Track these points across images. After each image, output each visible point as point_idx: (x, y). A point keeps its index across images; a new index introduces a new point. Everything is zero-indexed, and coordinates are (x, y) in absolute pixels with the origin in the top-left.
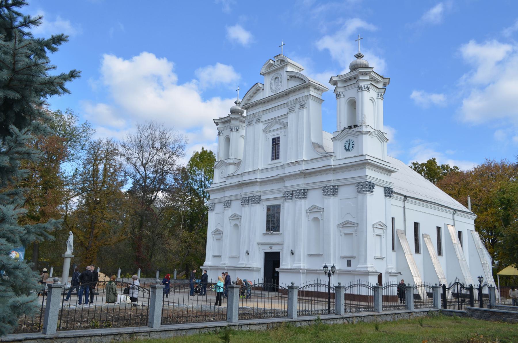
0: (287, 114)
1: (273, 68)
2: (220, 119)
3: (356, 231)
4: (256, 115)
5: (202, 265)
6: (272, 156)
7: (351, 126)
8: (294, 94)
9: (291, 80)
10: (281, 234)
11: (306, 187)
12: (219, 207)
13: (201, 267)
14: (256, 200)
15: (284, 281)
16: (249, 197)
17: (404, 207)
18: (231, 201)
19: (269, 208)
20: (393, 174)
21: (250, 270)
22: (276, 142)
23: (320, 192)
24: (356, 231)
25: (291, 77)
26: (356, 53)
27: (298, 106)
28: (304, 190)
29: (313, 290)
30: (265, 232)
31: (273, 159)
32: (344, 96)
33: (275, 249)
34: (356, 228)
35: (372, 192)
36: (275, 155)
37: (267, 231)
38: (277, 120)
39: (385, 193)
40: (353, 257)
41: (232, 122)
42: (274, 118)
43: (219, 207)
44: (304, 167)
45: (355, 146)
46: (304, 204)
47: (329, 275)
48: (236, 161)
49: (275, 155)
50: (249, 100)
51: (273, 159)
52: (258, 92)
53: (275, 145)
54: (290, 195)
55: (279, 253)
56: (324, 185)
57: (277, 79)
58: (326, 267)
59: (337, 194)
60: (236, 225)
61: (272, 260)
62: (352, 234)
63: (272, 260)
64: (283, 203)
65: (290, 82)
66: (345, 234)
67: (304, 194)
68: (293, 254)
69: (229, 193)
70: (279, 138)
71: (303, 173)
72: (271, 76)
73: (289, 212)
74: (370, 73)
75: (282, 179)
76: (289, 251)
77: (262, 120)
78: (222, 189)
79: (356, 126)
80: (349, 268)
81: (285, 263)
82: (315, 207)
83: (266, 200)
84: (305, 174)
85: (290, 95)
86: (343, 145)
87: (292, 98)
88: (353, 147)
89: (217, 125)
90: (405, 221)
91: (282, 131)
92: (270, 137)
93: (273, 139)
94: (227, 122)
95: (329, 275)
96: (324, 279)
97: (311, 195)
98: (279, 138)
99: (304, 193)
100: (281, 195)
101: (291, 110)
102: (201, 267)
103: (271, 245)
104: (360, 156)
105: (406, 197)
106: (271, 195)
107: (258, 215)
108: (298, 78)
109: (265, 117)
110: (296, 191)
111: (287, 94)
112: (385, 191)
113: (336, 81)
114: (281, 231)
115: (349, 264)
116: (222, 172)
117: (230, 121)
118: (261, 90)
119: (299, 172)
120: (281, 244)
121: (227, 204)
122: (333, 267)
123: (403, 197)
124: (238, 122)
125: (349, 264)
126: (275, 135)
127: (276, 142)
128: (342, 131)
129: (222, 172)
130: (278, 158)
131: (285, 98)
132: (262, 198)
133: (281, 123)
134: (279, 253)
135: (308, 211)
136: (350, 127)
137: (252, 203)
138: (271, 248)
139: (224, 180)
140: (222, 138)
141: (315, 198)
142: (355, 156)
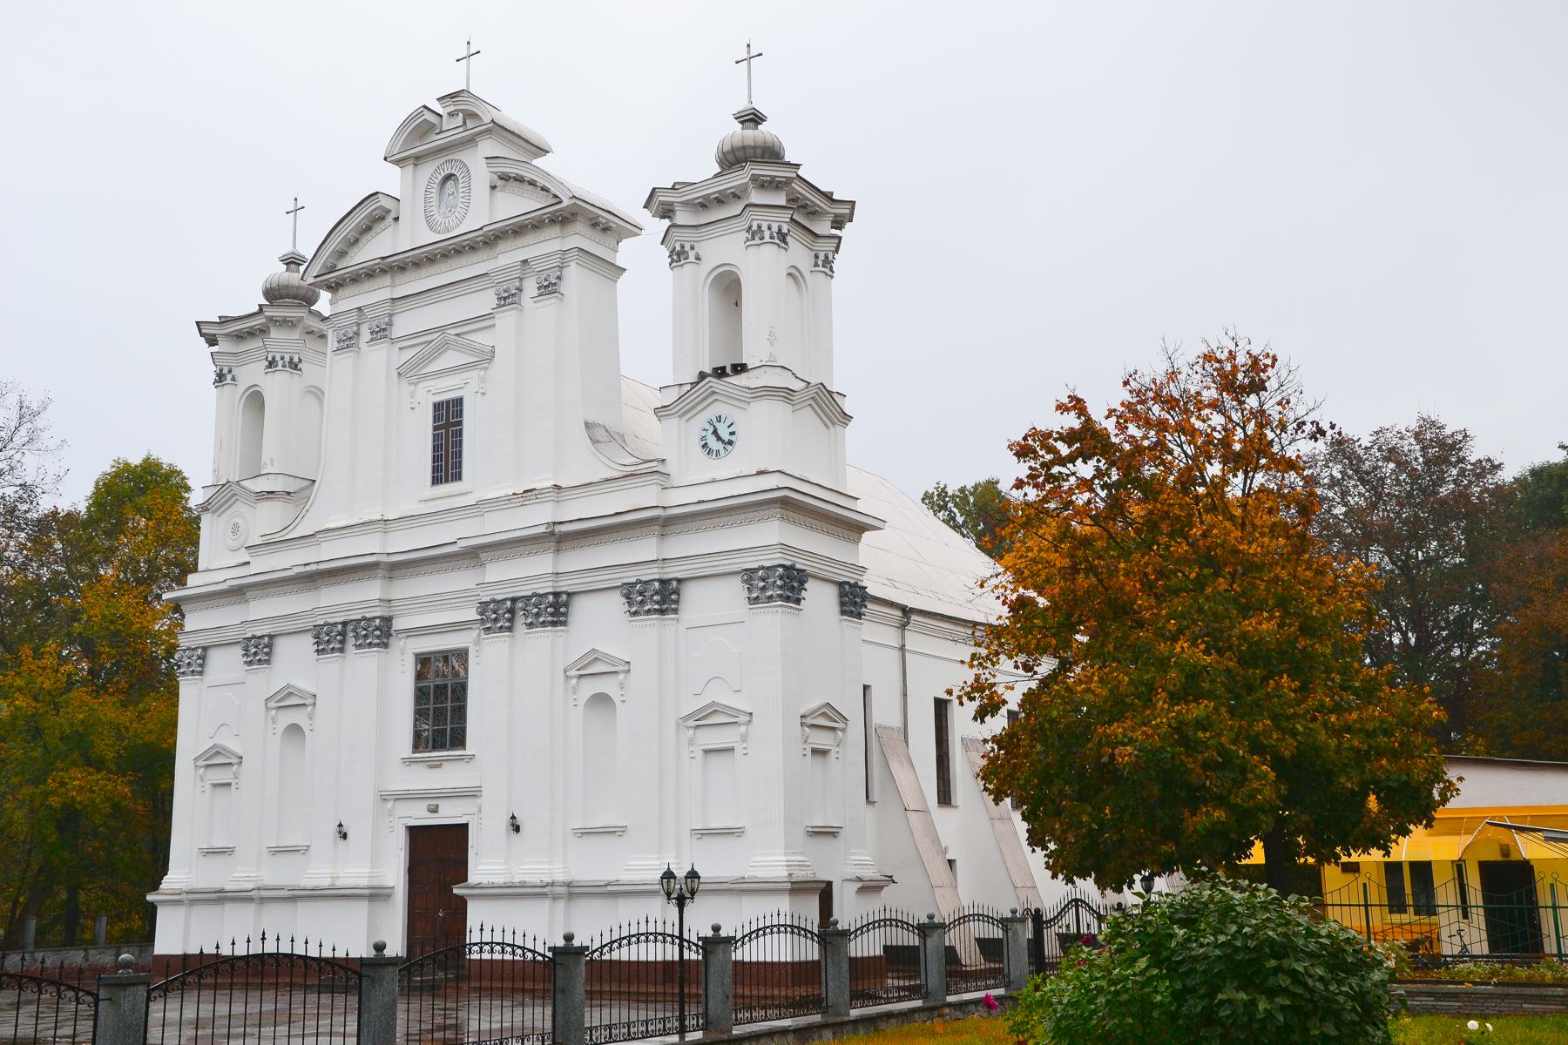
0: (490, 316)
1: (436, 141)
2: (224, 321)
3: (744, 738)
4: (370, 314)
5: (155, 887)
6: (435, 469)
7: (723, 369)
8: (520, 242)
10: (472, 757)
11: (565, 585)
12: (226, 664)
13: (150, 898)
16: (345, 624)
17: (902, 648)
18: (271, 637)
19: (423, 661)
20: (866, 535)
22: (448, 418)
24: (744, 738)
25: (505, 178)
26: (742, 105)
27: (531, 287)
28: (556, 595)
29: (625, 958)
31: (436, 481)
32: (698, 258)
33: (449, 814)
34: (743, 729)
35: (798, 601)
36: (447, 465)
37: (416, 747)
39: (842, 604)
41: (274, 333)
43: (226, 664)
47: (681, 903)
49: (447, 465)
50: (342, 254)
51: (436, 481)
52: (378, 228)
53: (448, 425)
54: (501, 615)
55: (464, 828)
56: (630, 576)
57: (450, 184)
58: (668, 875)
59: (675, 611)
60: (295, 729)
61: (438, 855)
62: (732, 749)
63: (438, 855)
64: (477, 642)
65: (500, 196)
66: (706, 752)
67: (554, 610)
68: (517, 829)
69: (263, 610)
70: (459, 402)
71: (552, 534)
72: (429, 170)
73: (500, 675)
74: (789, 181)
75: (473, 555)
76: (504, 822)
77: (398, 331)
78: (237, 593)
79: (740, 368)
82: (595, 657)
83: (412, 633)
84: (559, 539)
85: (502, 246)
86: (698, 433)
87: (508, 256)
89: (212, 341)
90: (905, 695)
91: (473, 375)
94: (251, 334)
95: (681, 903)
96: (661, 913)
98: (459, 402)
100: (472, 614)
101: (507, 299)
102: (150, 898)
103: (433, 799)
105: (907, 611)
106: (435, 611)
107: (383, 686)
108: (532, 183)
109: (406, 323)
110: (528, 598)
111: (490, 239)
112: (842, 595)
113: (672, 204)
114: (468, 752)
116: (236, 529)
117: (263, 331)
118: (389, 219)
119: (542, 529)
120: (472, 794)
122: (693, 875)
123: (899, 613)
124: (295, 335)
126: (444, 389)
127: (448, 418)
128: (694, 384)
129: (236, 529)
131: (483, 254)
132: (398, 624)
133: (470, 349)
134: (464, 828)
135: (573, 673)
136: (720, 373)
137: (359, 647)
138: (434, 810)
139: (244, 556)
140: (235, 394)
141: (601, 623)
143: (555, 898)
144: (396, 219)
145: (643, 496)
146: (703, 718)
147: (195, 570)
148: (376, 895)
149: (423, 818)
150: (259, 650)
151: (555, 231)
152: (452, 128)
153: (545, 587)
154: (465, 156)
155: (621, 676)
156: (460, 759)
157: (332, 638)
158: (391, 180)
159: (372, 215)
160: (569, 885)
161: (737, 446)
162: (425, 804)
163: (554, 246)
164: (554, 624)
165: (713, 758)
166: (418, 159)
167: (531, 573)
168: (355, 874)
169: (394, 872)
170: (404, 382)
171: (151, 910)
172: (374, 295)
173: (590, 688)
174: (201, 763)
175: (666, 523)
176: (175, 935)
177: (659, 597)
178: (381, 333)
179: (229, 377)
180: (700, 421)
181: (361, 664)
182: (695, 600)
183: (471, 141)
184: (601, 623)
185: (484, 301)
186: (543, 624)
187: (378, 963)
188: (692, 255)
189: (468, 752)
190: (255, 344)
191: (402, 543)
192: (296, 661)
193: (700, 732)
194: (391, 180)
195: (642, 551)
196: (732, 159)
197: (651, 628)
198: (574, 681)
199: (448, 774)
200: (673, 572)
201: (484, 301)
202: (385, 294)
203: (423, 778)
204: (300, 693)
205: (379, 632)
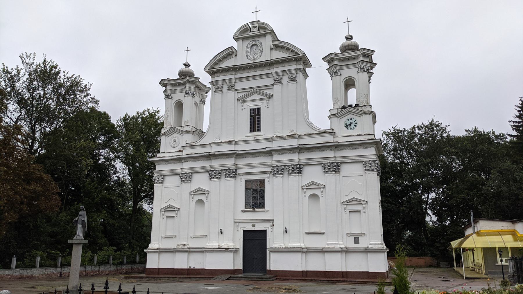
0: (273, 85)
3: (364, 208)
5: (147, 247)
9: (276, 50)
10: (268, 211)
11: (302, 162)
13: (145, 250)
15: (275, 263)
18: (192, 173)
24: (364, 208)
30: (243, 208)
33: (259, 227)
34: (364, 206)
40: (363, 235)
41: (188, 85)
42: (254, 88)
44: (303, 141)
45: (358, 125)
46: (293, 182)
48: (194, 130)
52: (229, 57)
53: (255, 115)
54: (278, 171)
55: (266, 231)
56: (326, 161)
57: (254, 47)
59: (339, 171)
60: (200, 201)
65: (274, 52)
66: (350, 212)
67: (298, 169)
68: (286, 232)
69: (186, 165)
72: (247, 43)
73: (275, 188)
75: (269, 153)
76: (282, 230)
80: (357, 246)
81: (273, 241)
84: (301, 149)
88: (355, 126)
91: (264, 102)
92: (248, 106)
93: (251, 110)
97: (306, 170)
99: (300, 168)
101: (278, 81)
102: (145, 250)
109: (239, 85)
110: (289, 166)
111: (271, 64)
114: (266, 209)
115: (357, 241)
117: (184, 84)
118: (234, 55)
120: (271, 221)
121: (186, 177)
125: (357, 241)
126: (255, 105)
130: (259, 130)
132: (239, 171)
133: (263, 94)
140: (172, 102)
141: (313, 174)
142: (360, 135)
143: (303, 252)
144: (236, 55)
145: (329, 139)
146: (349, 202)
147: (159, 152)
148: (236, 251)
149: (249, 227)
150: (186, 177)
151: (295, 63)
152: (255, 31)
153: (296, 163)
154: (262, 40)
155: (322, 189)
156: (264, 211)
157: (213, 175)
158: (235, 45)
159: (229, 53)
160: (306, 248)
162: (251, 224)
163: (294, 67)
164: (298, 173)
165: (352, 214)
166: (244, 39)
167: (292, 158)
168: (230, 244)
169: (239, 245)
170: (239, 102)
171: (145, 254)
174: (163, 210)
175: (337, 147)
176: (153, 262)
177: (334, 168)
178: (231, 88)
180: (344, 119)
182: (345, 169)
183: (264, 35)
184: (313, 174)
185: (270, 81)
186: (295, 173)
187: (235, 271)
188: (339, 73)
189: (266, 209)
191: (241, 148)
192: (201, 181)
193: (348, 206)
194: (235, 45)
195: (330, 154)
196: (344, 49)
198: (305, 190)
200: (339, 160)
202: (233, 76)
204: (203, 190)
205: (232, 173)
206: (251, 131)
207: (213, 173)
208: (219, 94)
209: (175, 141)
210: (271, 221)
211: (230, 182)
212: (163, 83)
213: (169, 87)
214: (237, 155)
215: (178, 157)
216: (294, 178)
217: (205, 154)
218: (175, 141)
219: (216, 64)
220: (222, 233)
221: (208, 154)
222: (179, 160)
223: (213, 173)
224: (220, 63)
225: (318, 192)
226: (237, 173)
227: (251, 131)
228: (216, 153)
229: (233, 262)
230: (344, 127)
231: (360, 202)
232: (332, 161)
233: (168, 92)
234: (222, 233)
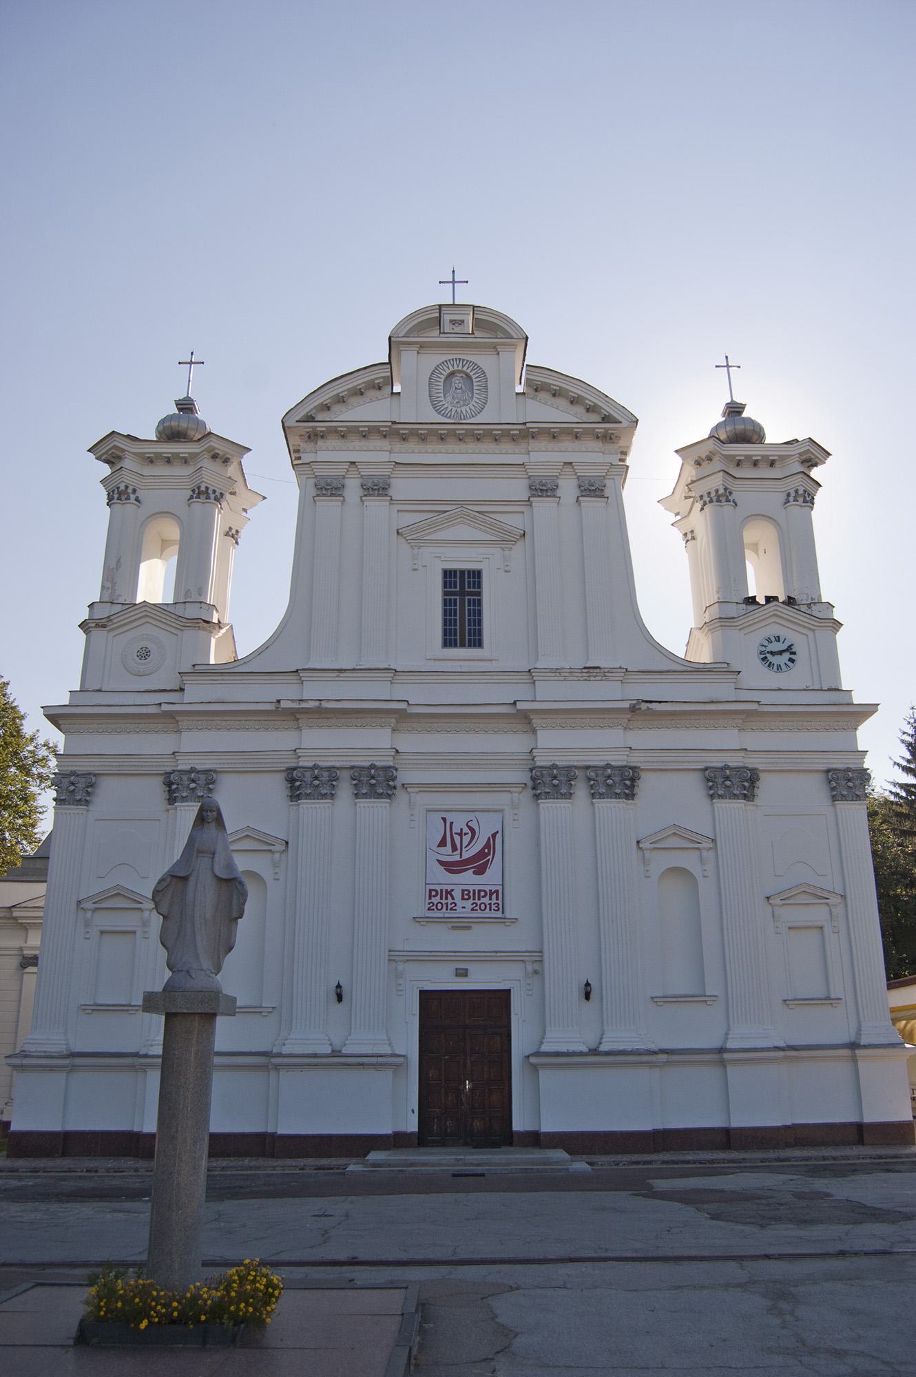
11: (635, 760)
14: (377, 782)
15: (544, 1103)
21: (375, 1066)
23: (693, 786)
33: (482, 979)
38: (477, 512)
52: (372, 393)
53: (462, 593)
54: (548, 782)
56: (716, 761)
67: (621, 782)
75: (524, 719)
76: (576, 992)
84: (638, 712)
87: (544, 457)
101: (543, 489)
103: (462, 964)
104: (829, 690)
111: (525, 434)
126: (463, 560)
132: (404, 777)
141: (671, 799)
145: (721, 689)
149: (443, 980)
153: (618, 760)
156: (503, 920)
161: (798, 663)
170: (402, 540)
172: (374, 455)
173: (663, 861)
178: (377, 488)
179: (133, 497)
181: (342, 810)
186: (617, 796)
190: (179, 470)
191: (416, 695)
197: (731, 808)
199: (482, 938)
201: (517, 489)
202: (384, 457)
203: (443, 939)
206: (447, 643)
207: (308, 778)
208: (329, 506)
209: (144, 654)
210: (535, 961)
211: (374, 809)
212: (110, 450)
213: (128, 463)
214: (402, 717)
215: (165, 707)
216: (610, 808)
217: (284, 705)
218: (144, 654)
219: (340, 400)
220: (340, 998)
221: (295, 705)
222: (170, 720)
223: (308, 778)
224: (336, 408)
225: (688, 861)
226: (398, 783)
227: (447, 643)
228: (325, 704)
229: (394, 1107)
230: (758, 662)
231: (821, 896)
232: (734, 760)
233: (128, 479)
234: (340, 998)
